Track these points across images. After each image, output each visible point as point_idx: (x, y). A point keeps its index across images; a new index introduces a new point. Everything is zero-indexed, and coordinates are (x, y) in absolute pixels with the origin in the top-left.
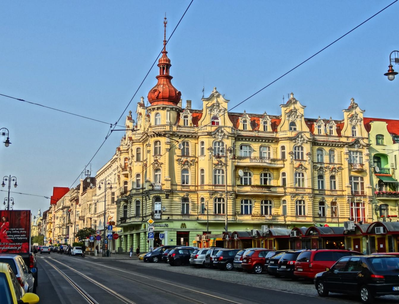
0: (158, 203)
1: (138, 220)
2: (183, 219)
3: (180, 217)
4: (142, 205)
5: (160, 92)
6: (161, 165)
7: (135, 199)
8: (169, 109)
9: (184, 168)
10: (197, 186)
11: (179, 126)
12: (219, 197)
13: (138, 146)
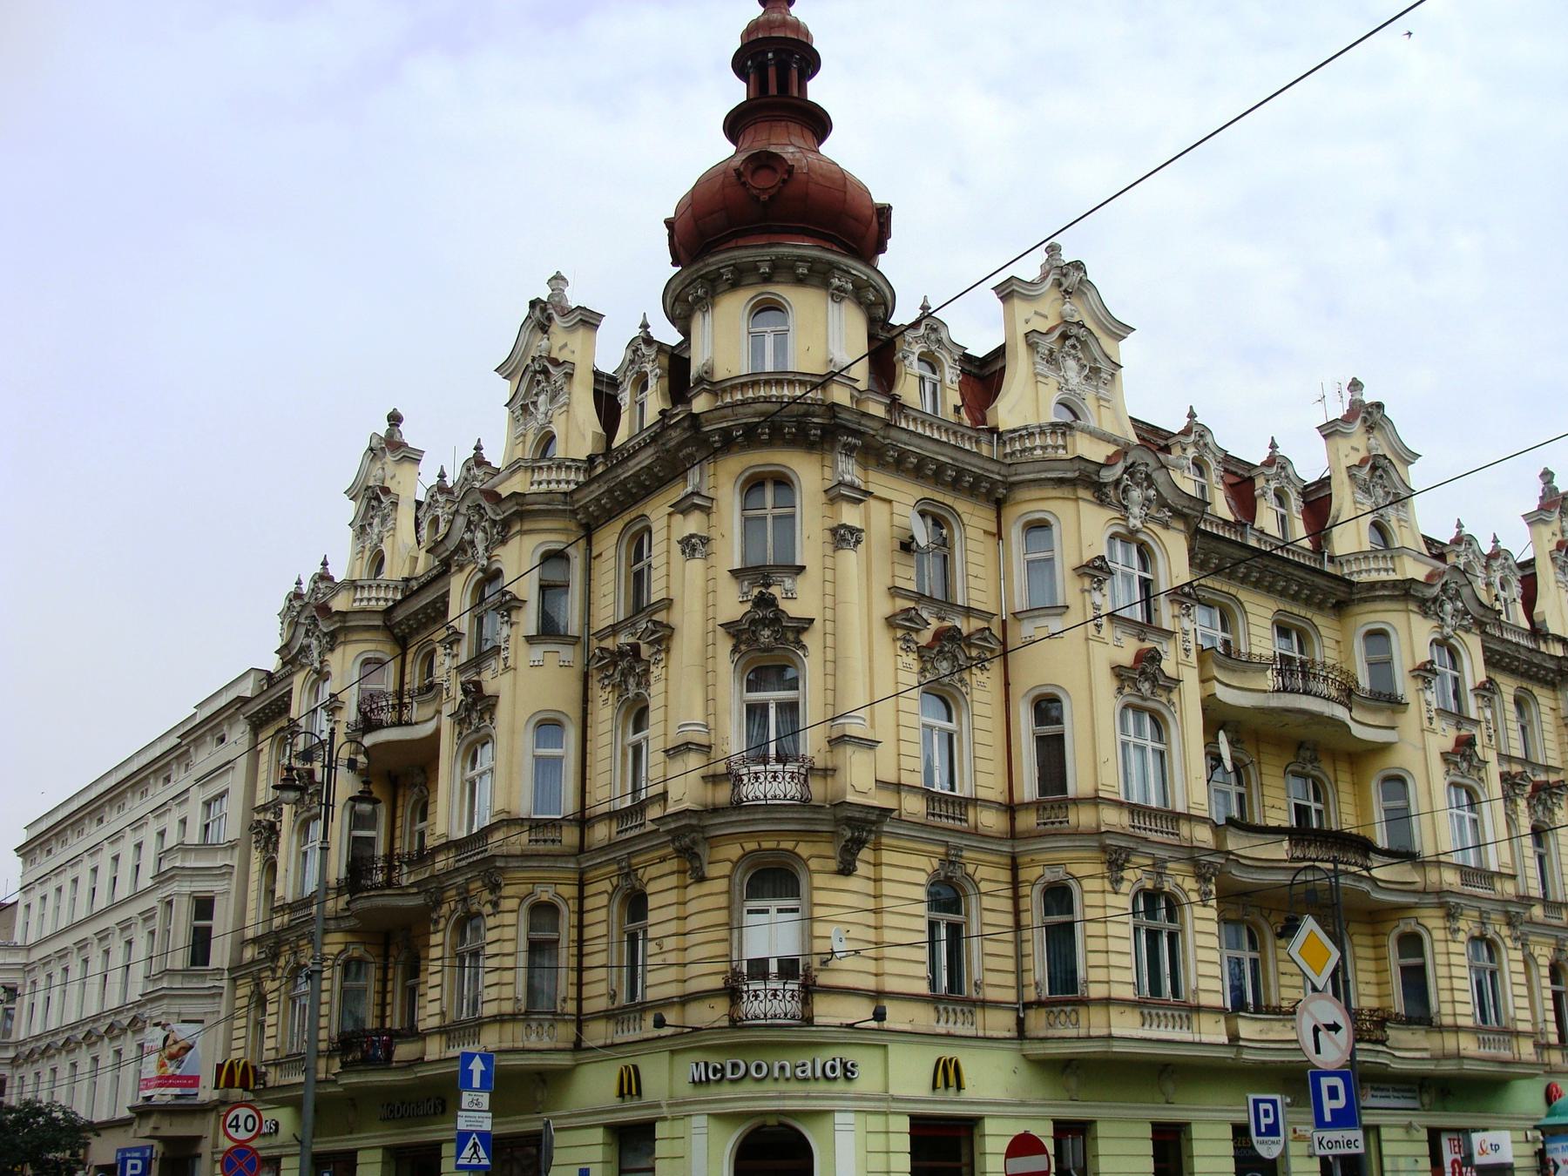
0: (774, 904)
1: (546, 1043)
2: (941, 1028)
3: (923, 1017)
4: (574, 934)
7: (523, 889)
8: (850, 286)
11: (896, 405)
12: (1149, 885)
13: (555, 541)
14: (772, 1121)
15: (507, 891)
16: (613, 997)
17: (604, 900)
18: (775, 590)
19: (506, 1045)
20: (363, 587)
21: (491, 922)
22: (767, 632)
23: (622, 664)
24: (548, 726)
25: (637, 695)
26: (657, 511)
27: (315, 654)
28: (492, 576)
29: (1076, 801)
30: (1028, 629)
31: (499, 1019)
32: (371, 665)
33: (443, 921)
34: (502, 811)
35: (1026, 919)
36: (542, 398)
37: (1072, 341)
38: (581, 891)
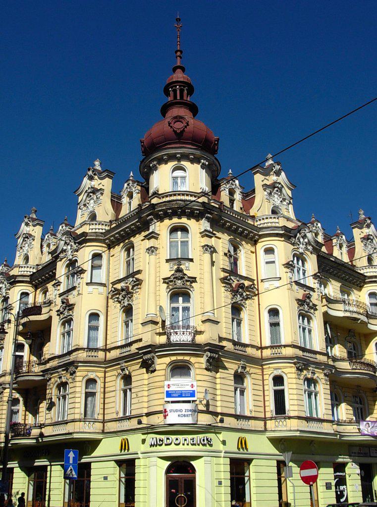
1: (91, 430)
5: (188, 125)
6: (191, 283)
7: (85, 373)
9: (234, 301)
10: (262, 348)
12: (309, 376)
13: (98, 250)
14: (181, 460)
15: (78, 374)
16: (117, 413)
18: (182, 266)
19: (78, 430)
20: (22, 267)
21: (71, 385)
22: (179, 282)
23: (124, 292)
24: (94, 316)
25: (129, 304)
26: (137, 240)
27: (4, 290)
28: (72, 263)
29: (285, 346)
30: (266, 285)
31: (73, 421)
32: (25, 294)
34: (77, 345)
35: (266, 388)
36: (92, 201)
37: (276, 189)
38: (105, 375)
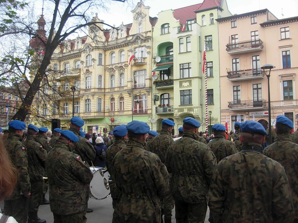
15: (95, 97)
17: (108, 99)
33: (83, 100)
